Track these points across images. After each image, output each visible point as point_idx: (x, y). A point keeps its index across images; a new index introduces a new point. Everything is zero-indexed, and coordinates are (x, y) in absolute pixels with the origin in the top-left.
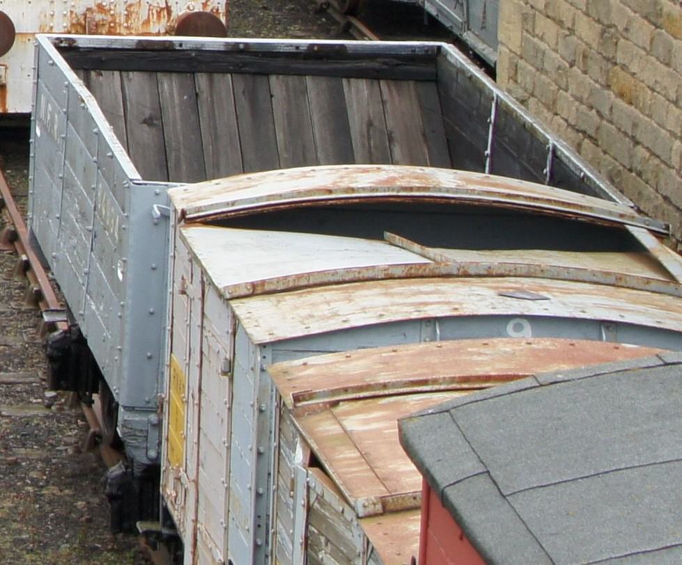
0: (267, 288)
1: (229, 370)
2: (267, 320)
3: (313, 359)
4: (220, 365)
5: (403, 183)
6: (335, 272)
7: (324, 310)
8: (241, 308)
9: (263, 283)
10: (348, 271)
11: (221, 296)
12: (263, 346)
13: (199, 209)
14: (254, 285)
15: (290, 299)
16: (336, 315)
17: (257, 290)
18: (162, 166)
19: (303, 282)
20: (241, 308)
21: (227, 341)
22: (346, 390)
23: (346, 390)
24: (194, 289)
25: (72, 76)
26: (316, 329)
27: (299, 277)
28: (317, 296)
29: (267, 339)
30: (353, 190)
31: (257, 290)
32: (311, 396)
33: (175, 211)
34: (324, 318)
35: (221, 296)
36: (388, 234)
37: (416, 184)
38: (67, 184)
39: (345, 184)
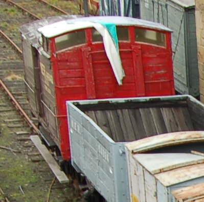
0: (165, 170)
1: (156, 195)
2: (168, 179)
3: (184, 189)
4: (153, 194)
5: (193, 137)
6: (183, 164)
7: (182, 175)
8: (158, 177)
9: (163, 169)
10: (187, 163)
11: (150, 173)
12: (167, 187)
13: (137, 150)
14: (160, 170)
15: (172, 173)
16: (186, 176)
17: (162, 171)
18: (120, 137)
19: (174, 167)
20: (158, 177)
21: (154, 187)
22: (197, 196)
23: (197, 196)
24: (140, 172)
25: (82, 113)
26: (182, 180)
27: (173, 166)
28: (179, 171)
29: (168, 185)
30: (180, 140)
31: (162, 171)
32: (187, 199)
33: (129, 150)
34: (183, 177)
35: (150, 173)
36: (192, 152)
37: (197, 136)
38: (85, 146)
39: (177, 138)
